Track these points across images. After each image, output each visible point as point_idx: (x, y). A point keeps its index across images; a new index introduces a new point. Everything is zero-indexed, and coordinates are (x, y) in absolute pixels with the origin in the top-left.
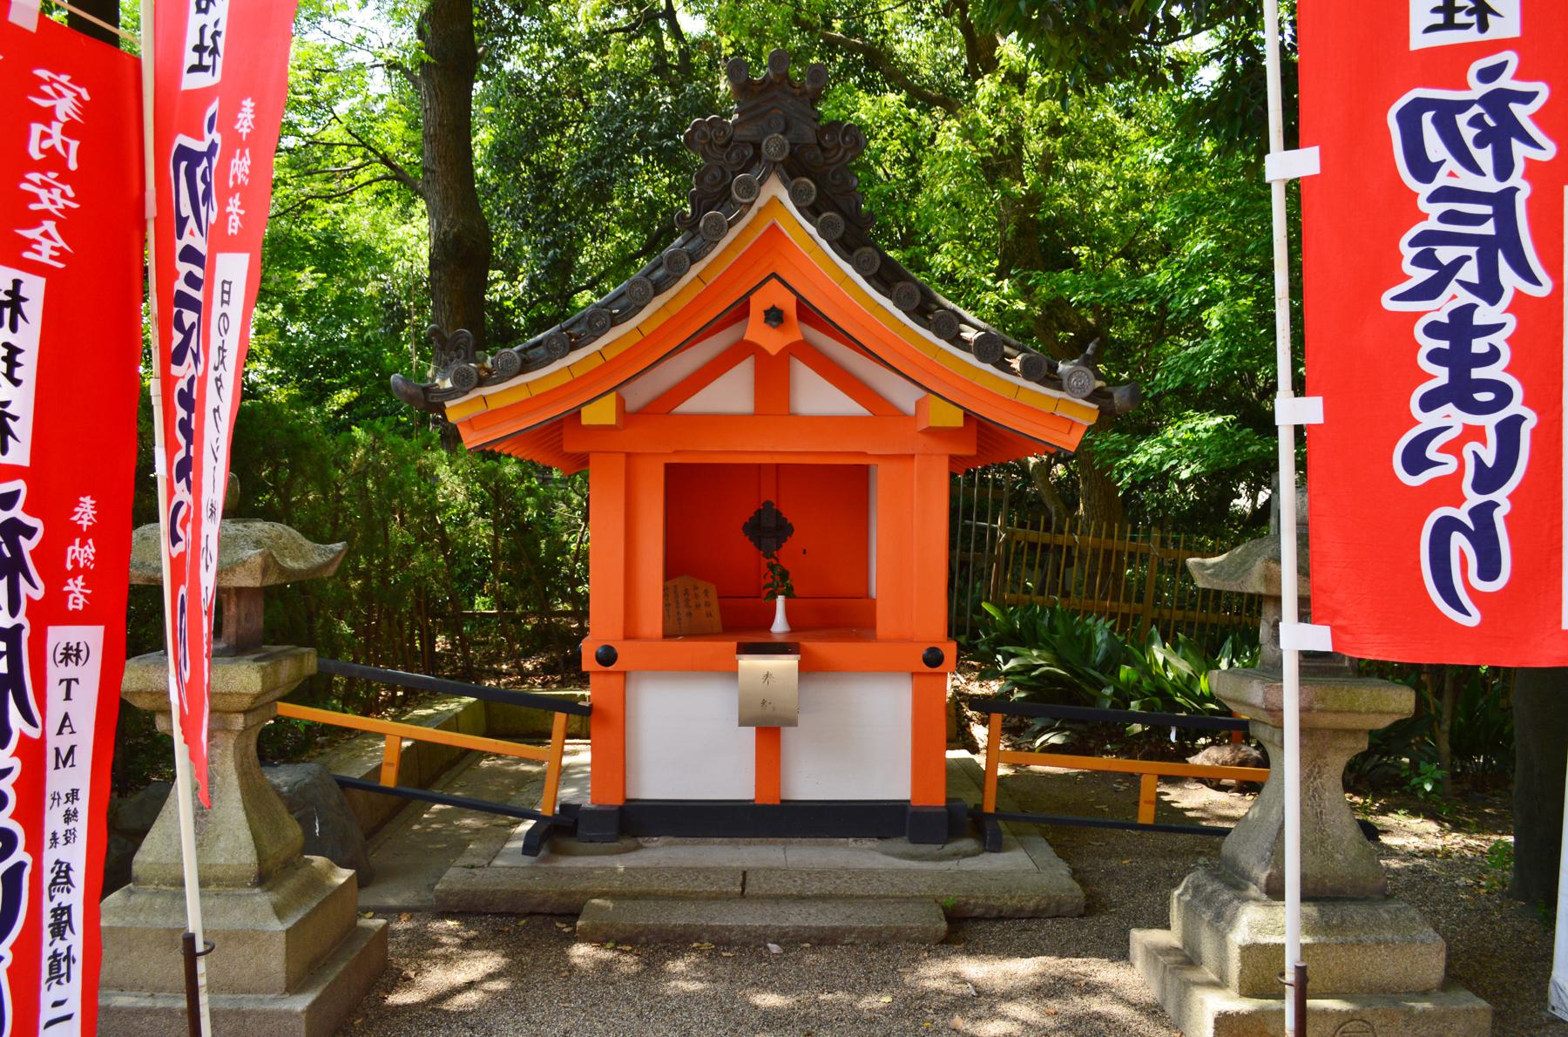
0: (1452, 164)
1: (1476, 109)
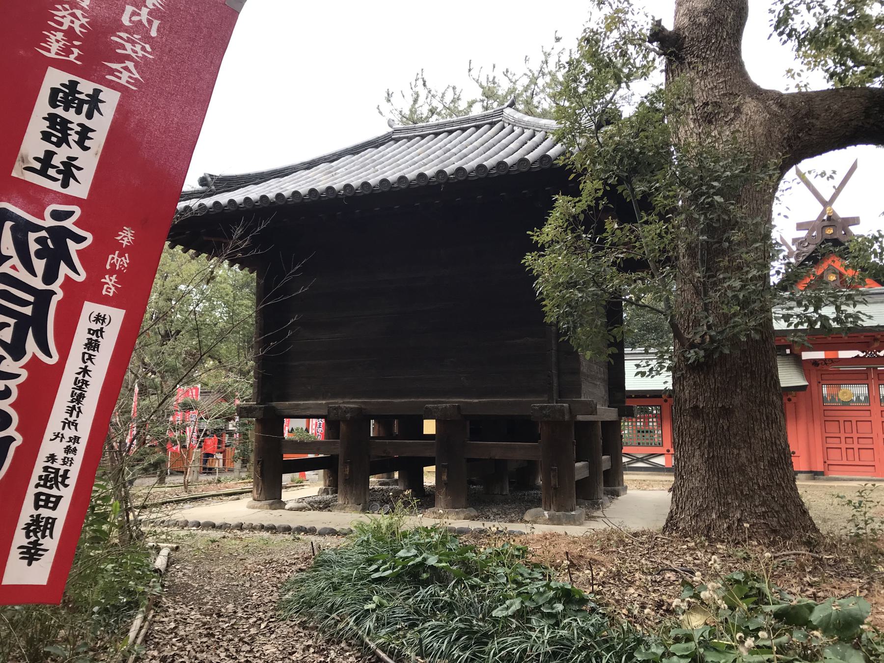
0: (16, 261)
1: (44, 234)
